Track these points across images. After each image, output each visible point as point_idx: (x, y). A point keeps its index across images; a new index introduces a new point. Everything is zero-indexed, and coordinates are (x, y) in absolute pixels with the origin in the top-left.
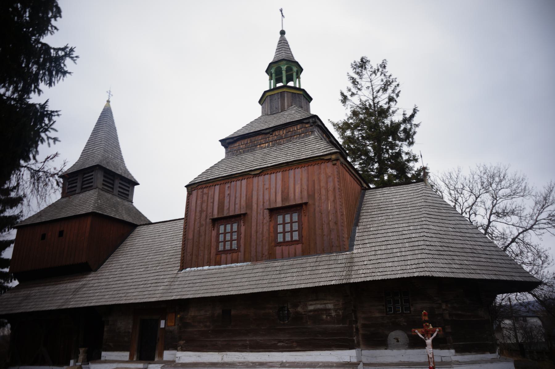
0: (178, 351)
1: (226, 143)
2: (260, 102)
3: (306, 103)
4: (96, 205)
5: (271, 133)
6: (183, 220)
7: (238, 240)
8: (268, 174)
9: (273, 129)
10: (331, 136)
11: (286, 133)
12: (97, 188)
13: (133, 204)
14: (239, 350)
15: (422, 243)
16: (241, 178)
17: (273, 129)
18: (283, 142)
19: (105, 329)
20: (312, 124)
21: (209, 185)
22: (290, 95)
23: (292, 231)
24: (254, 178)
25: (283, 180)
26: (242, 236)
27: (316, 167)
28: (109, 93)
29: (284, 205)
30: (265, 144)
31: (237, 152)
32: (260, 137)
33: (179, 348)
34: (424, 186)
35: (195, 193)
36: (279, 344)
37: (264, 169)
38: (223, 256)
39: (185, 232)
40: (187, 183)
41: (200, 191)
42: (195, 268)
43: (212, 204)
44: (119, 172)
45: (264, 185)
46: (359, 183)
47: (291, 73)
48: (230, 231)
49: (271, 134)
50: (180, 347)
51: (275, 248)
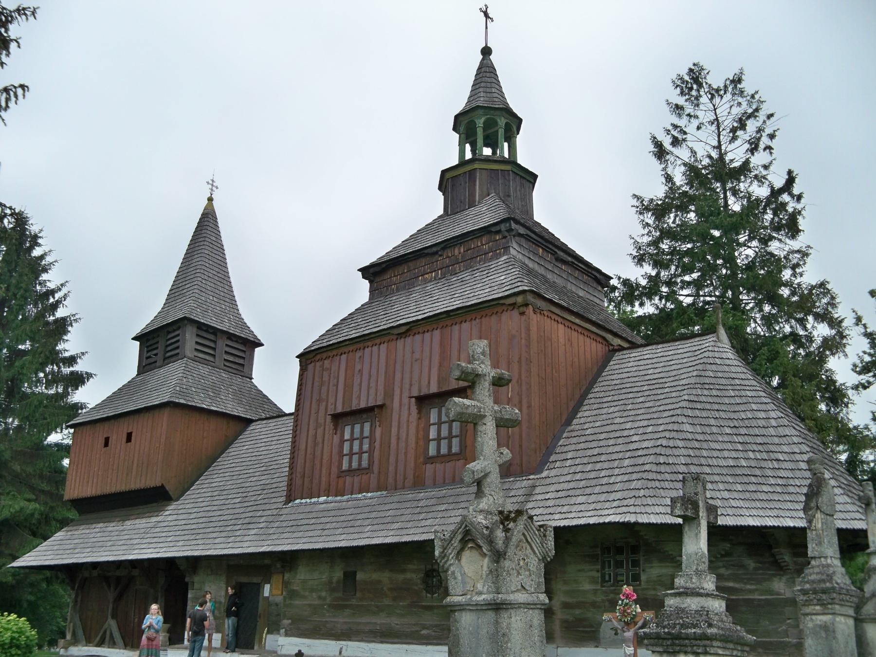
0: (281, 636)
1: (370, 272)
2: (440, 188)
3: (522, 186)
4: (178, 388)
5: (440, 253)
6: (293, 417)
7: (371, 451)
8: (419, 333)
9: (442, 245)
11: (464, 251)
12: (185, 357)
13: (253, 380)
14: (364, 638)
15: (652, 459)
16: (378, 341)
17: (442, 245)
18: (460, 269)
19: (190, 596)
20: (506, 234)
21: (330, 354)
22: (484, 172)
23: (450, 437)
24: (398, 341)
25: (442, 344)
26: (377, 444)
27: (494, 318)
28: (212, 184)
29: (441, 390)
30: (430, 274)
31: (387, 289)
32: (423, 261)
33: (282, 631)
34: (712, 344)
35: (311, 367)
36: (424, 632)
37: (412, 325)
38: (348, 479)
39: (294, 437)
40: (300, 351)
41: (318, 364)
42: (308, 500)
43: (335, 387)
44: (224, 326)
45: (413, 352)
46: (599, 339)
47: (495, 129)
48: (359, 436)
49: (441, 256)
50: (284, 630)
51: (424, 466)
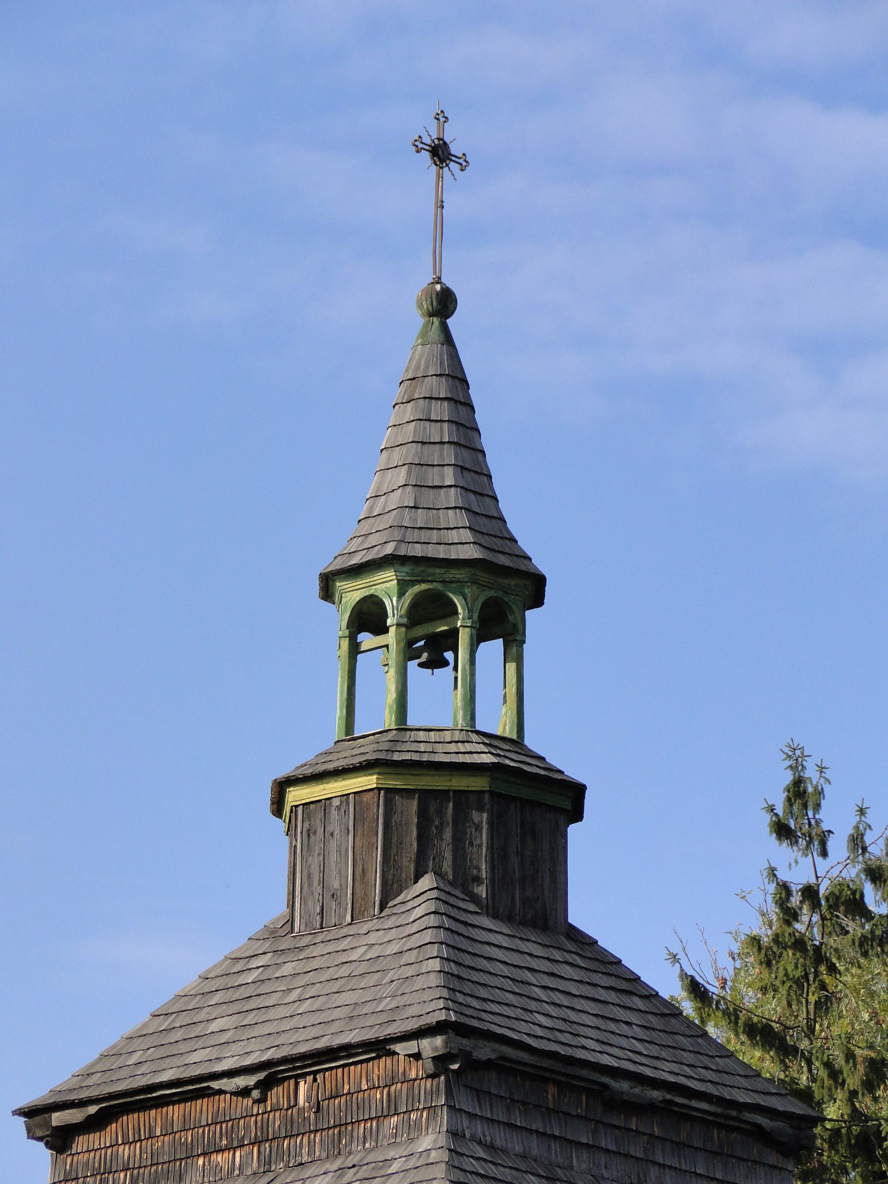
5: (256, 1094)
10: (606, 1080)
17: (261, 1075)
